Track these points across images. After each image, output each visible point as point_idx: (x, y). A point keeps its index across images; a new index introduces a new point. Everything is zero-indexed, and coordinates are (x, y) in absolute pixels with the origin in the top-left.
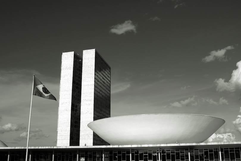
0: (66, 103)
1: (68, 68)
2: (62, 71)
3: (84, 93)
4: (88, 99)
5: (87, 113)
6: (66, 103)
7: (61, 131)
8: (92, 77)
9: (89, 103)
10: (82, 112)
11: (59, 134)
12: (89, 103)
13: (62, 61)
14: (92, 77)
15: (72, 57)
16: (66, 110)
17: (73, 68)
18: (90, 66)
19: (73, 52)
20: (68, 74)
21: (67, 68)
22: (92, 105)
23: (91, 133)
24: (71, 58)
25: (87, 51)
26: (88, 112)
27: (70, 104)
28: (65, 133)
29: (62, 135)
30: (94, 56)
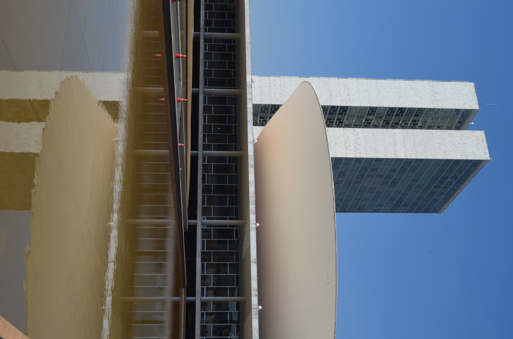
1: (435, 97)
4: (358, 144)
6: (348, 95)
7: (280, 85)
9: (349, 146)
11: (274, 81)
13: (453, 83)
17: (436, 107)
18: (443, 147)
19: (478, 108)
20: (420, 98)
21: (436, 95)
22: (346, 153)
25: (482, 139)
27: (346, 103)
30: (470, 158)
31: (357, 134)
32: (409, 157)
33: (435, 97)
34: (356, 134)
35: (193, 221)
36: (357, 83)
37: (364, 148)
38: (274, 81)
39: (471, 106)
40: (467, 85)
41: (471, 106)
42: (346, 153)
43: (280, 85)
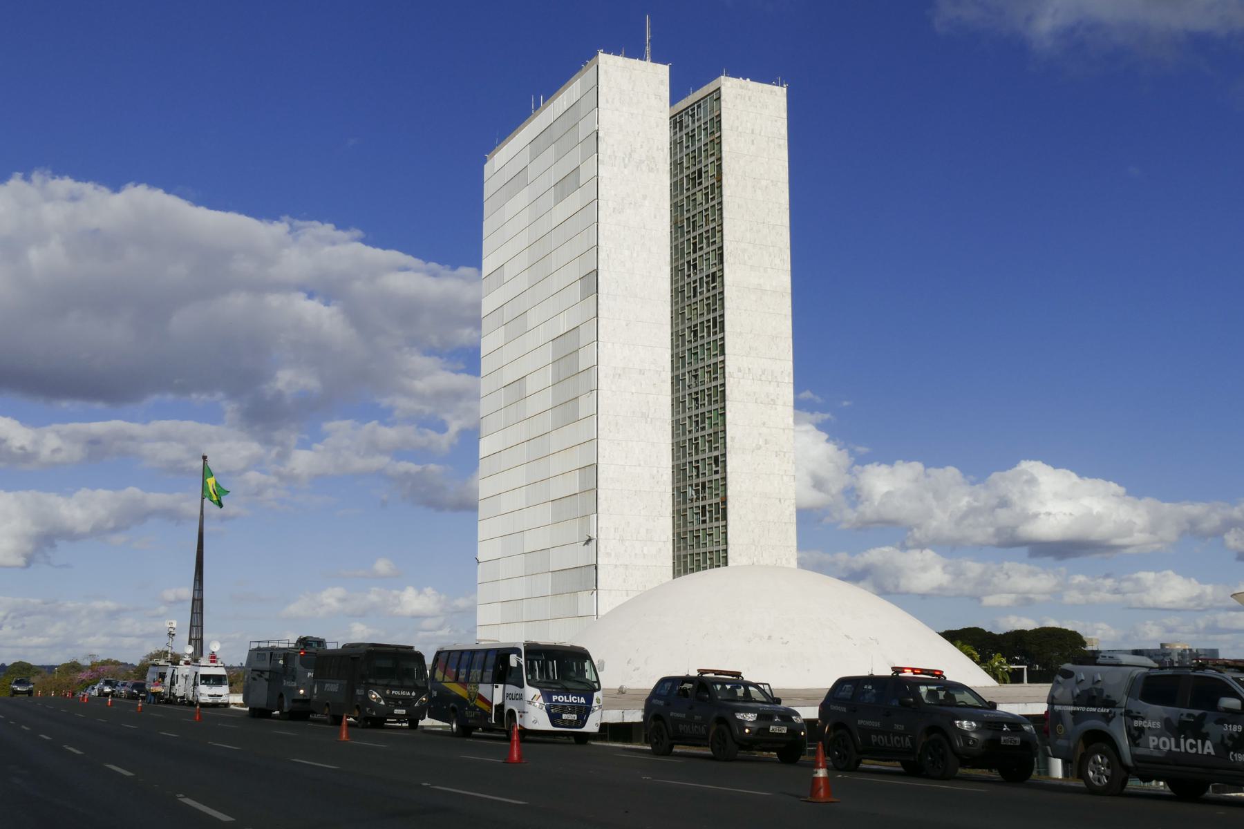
0: (641, 372)
1: (642, 162)
3: (741, 334)
5: (759, 448)
6: (641, 372)
7: (622, 540)
9: (767, 395)
11: (609, 554)
12: (767, 395)
18: (764, 183)
20: (645, 197)
22: (784, 404)
25: (742, 87)
26: (766, 442)
27: (663, 381)
29: (626, 566)
31: (740, 371)
32: (788, 266)
33: (642, 162)
34: (741, 375)
36: (609, 345)
38: (609, 554)
39: (662, 82)
40: (606, 72)
41: (662, 82)
42: (784, 404)
43: (622, 540)
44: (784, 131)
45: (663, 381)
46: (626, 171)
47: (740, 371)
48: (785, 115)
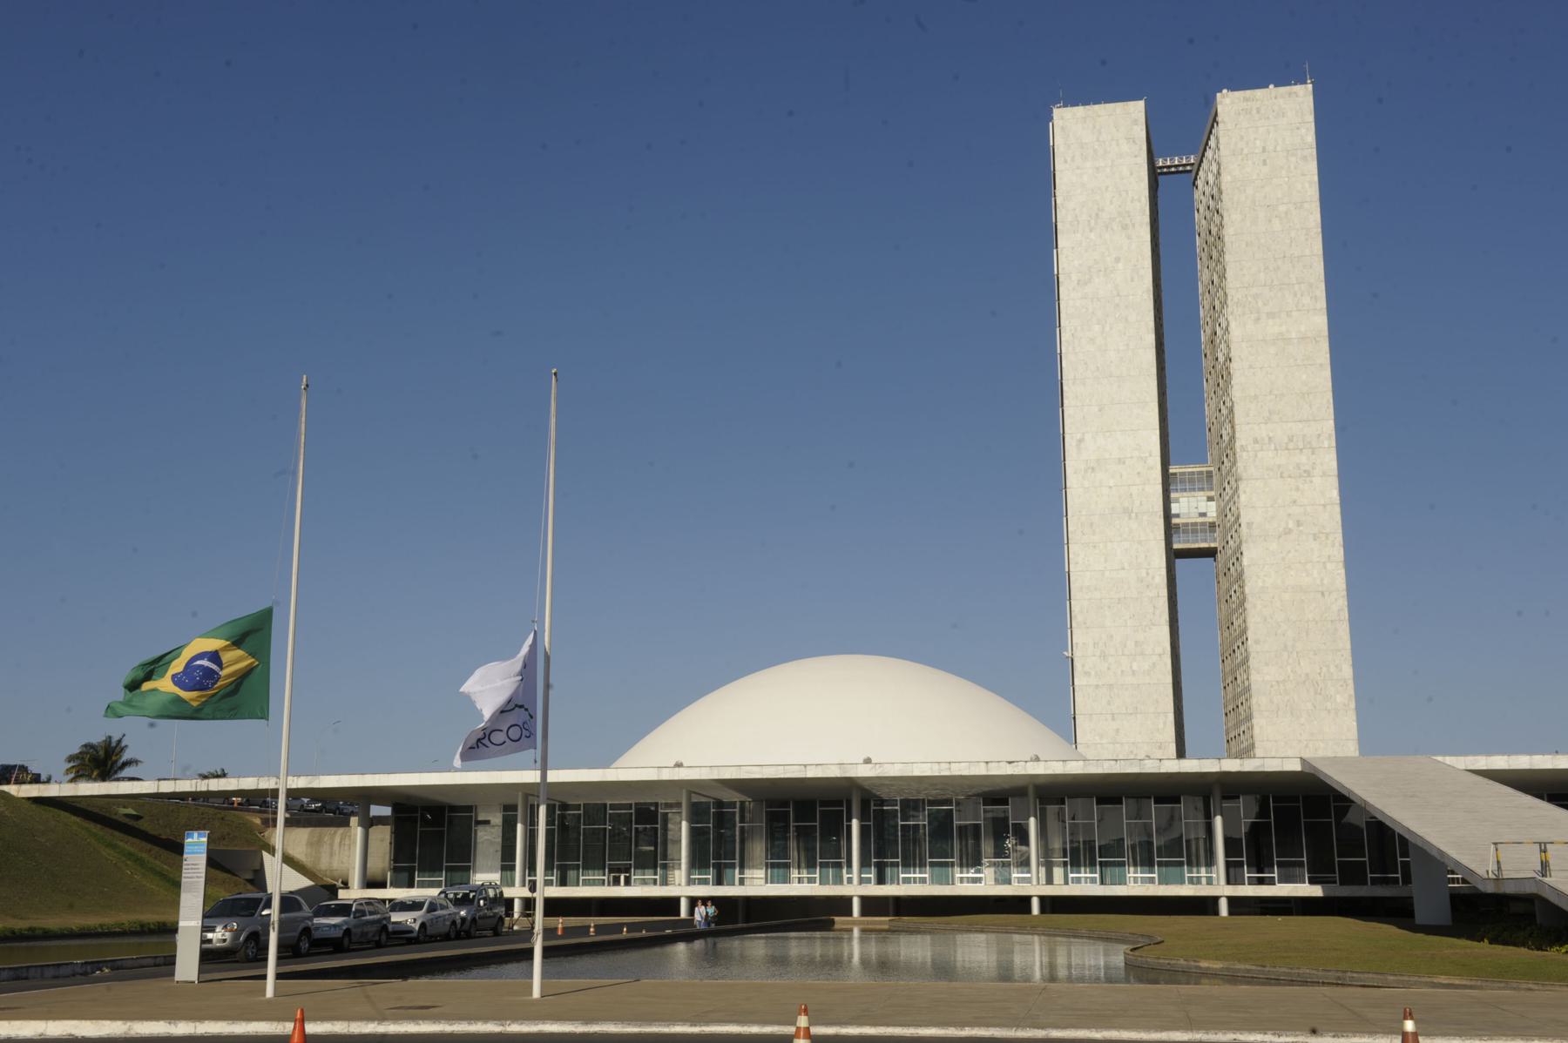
0: (1121, 461)
2: (1066, 242)
3: (1256, 397)
4: (1291, 440)
5: (1288, 532)
6: (1121, 461)
8: (1311, 285)
9: (1298, 466)
10: (1249, 525)
14: (1311, 285)
15: (1131, 140)
16: (1127, 512)
18: (1282, 208)
20: (1118, 260)
22: (1324, 474)
23: (1332, 669)
24: (1125, 147)
25: (1246, 100)
26: (1299, 524)
27: (1151, 468)
28: (1134, 672)
29: (1111, 686)
31: (1256, 441)
32: (1322, 304)
34: (1257, 446)
35: (1035, 904)
37: (1300, 425)
38: (1087, 674)
41: (1135, 122)
42: (1324, 474)
43: (1104, 656)
44: (1311, 138)
45: (1151, 468)
46: (1092, 236)
47: (1256, 441)
48: (1311, 118)
